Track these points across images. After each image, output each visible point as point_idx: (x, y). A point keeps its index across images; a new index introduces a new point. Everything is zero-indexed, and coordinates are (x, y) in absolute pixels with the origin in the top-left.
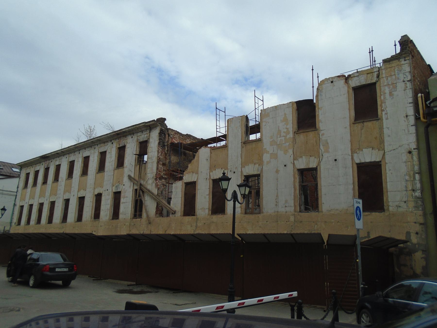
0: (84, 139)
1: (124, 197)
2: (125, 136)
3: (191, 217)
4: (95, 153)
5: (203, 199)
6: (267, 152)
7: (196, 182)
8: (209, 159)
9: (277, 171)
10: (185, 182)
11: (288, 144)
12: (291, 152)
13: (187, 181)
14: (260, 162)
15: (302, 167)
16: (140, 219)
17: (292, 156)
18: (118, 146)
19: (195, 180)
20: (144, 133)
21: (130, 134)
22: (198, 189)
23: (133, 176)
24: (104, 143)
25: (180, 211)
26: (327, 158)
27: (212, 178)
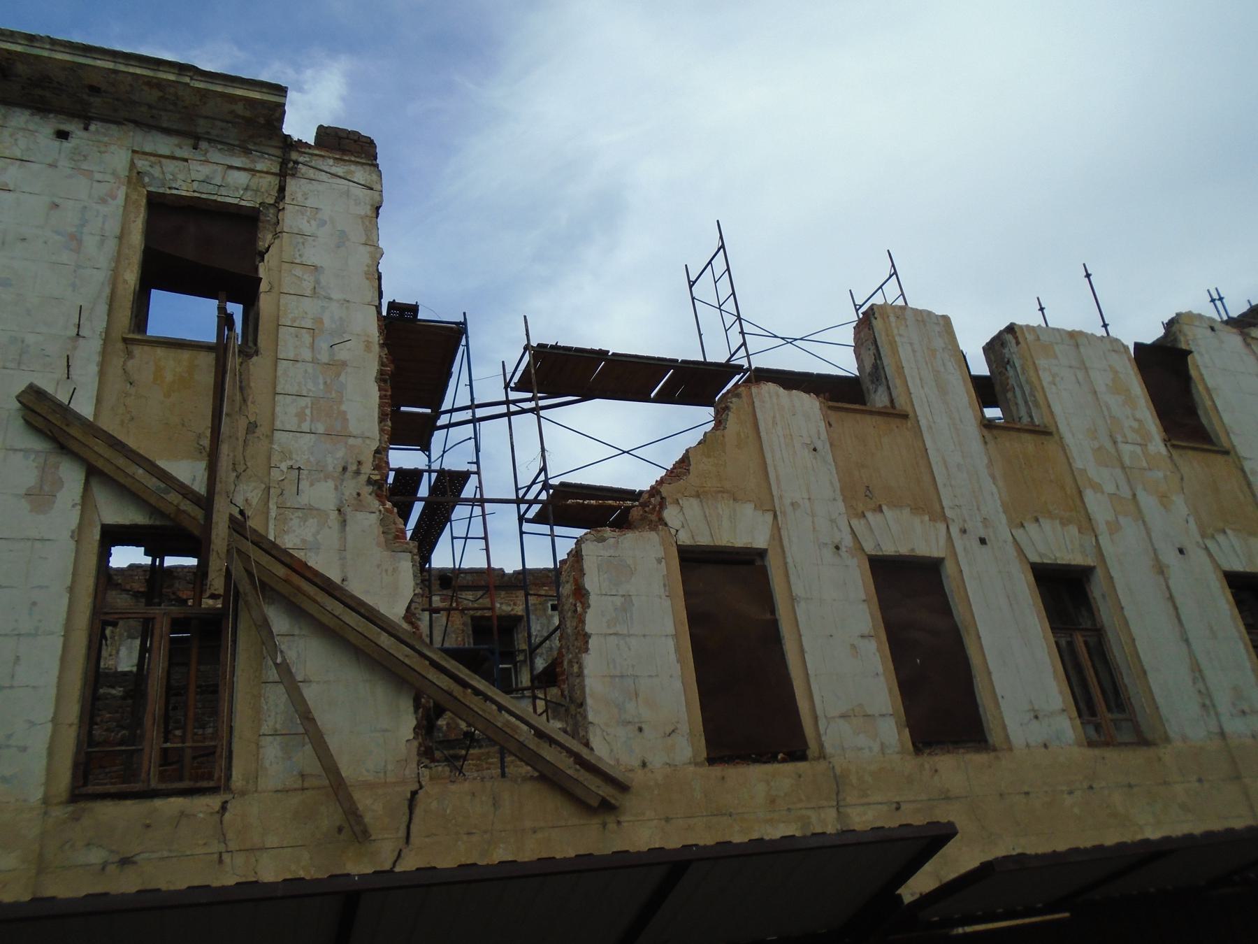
3: (789, 767)
5: (839, 659)
6: (1097, 488)
7: (762, 553)
8: (824, 448)
9: (1161, 569)
10: (684, 539)
11: (1160, 474)
13: (704, 540)
16: (214, 802)
17: (1191, 520)
19: (760, 542)
20: (215, 156)
21: (41, 107)
22: (793, 599)
23: (84, 407)
25: (684, 728)
27: (870, 548)
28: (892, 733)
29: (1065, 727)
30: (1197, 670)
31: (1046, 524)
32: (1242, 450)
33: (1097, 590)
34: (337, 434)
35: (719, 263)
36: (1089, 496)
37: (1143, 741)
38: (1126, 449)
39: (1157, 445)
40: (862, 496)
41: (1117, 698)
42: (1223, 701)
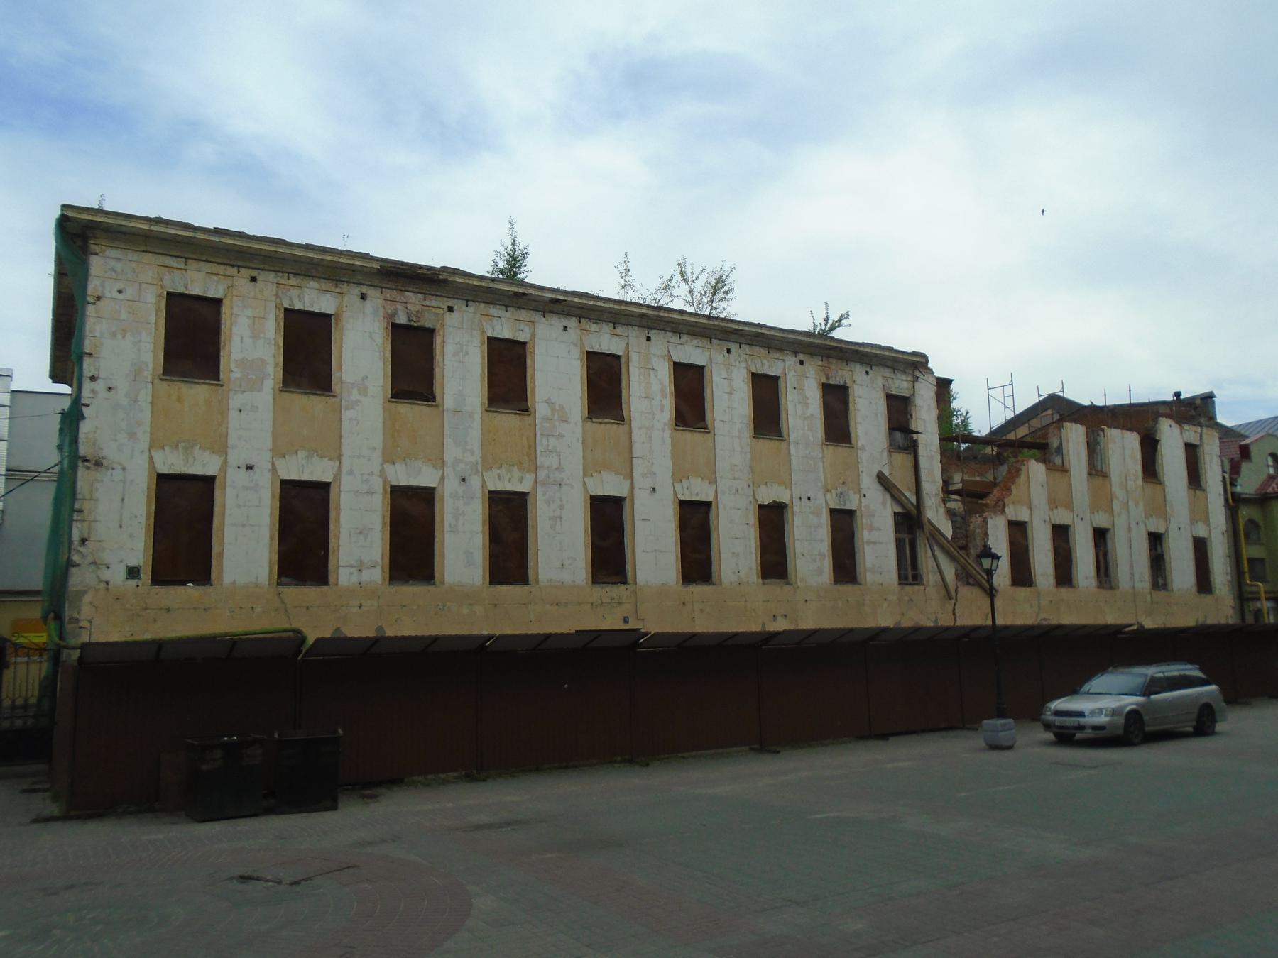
0: (679, 301)
1: (871, 529)
2: (847, 361)
4: (729, 366)
9: (1129, 530)
12: (1141, 504)
14: (1111, 511)
15: (1153, 530)
18: (824, 380)
21: (861, 362)
24: (769, 348)
26: (1173, 526)
28: (1052, 581)
29: (1093, 582)
30: (1132, 567)
31: (1101, 513)
32: (1167, 483)
33: (1109, 536)
34: (934, 482)
35: (1008, 390)
36: (1115, 502)
37: (1111, 588)
38: (1130, 483)
39: (1140, 482)
40: (1053, 504)
41: (1107, 574)
42: (1136, 577)
